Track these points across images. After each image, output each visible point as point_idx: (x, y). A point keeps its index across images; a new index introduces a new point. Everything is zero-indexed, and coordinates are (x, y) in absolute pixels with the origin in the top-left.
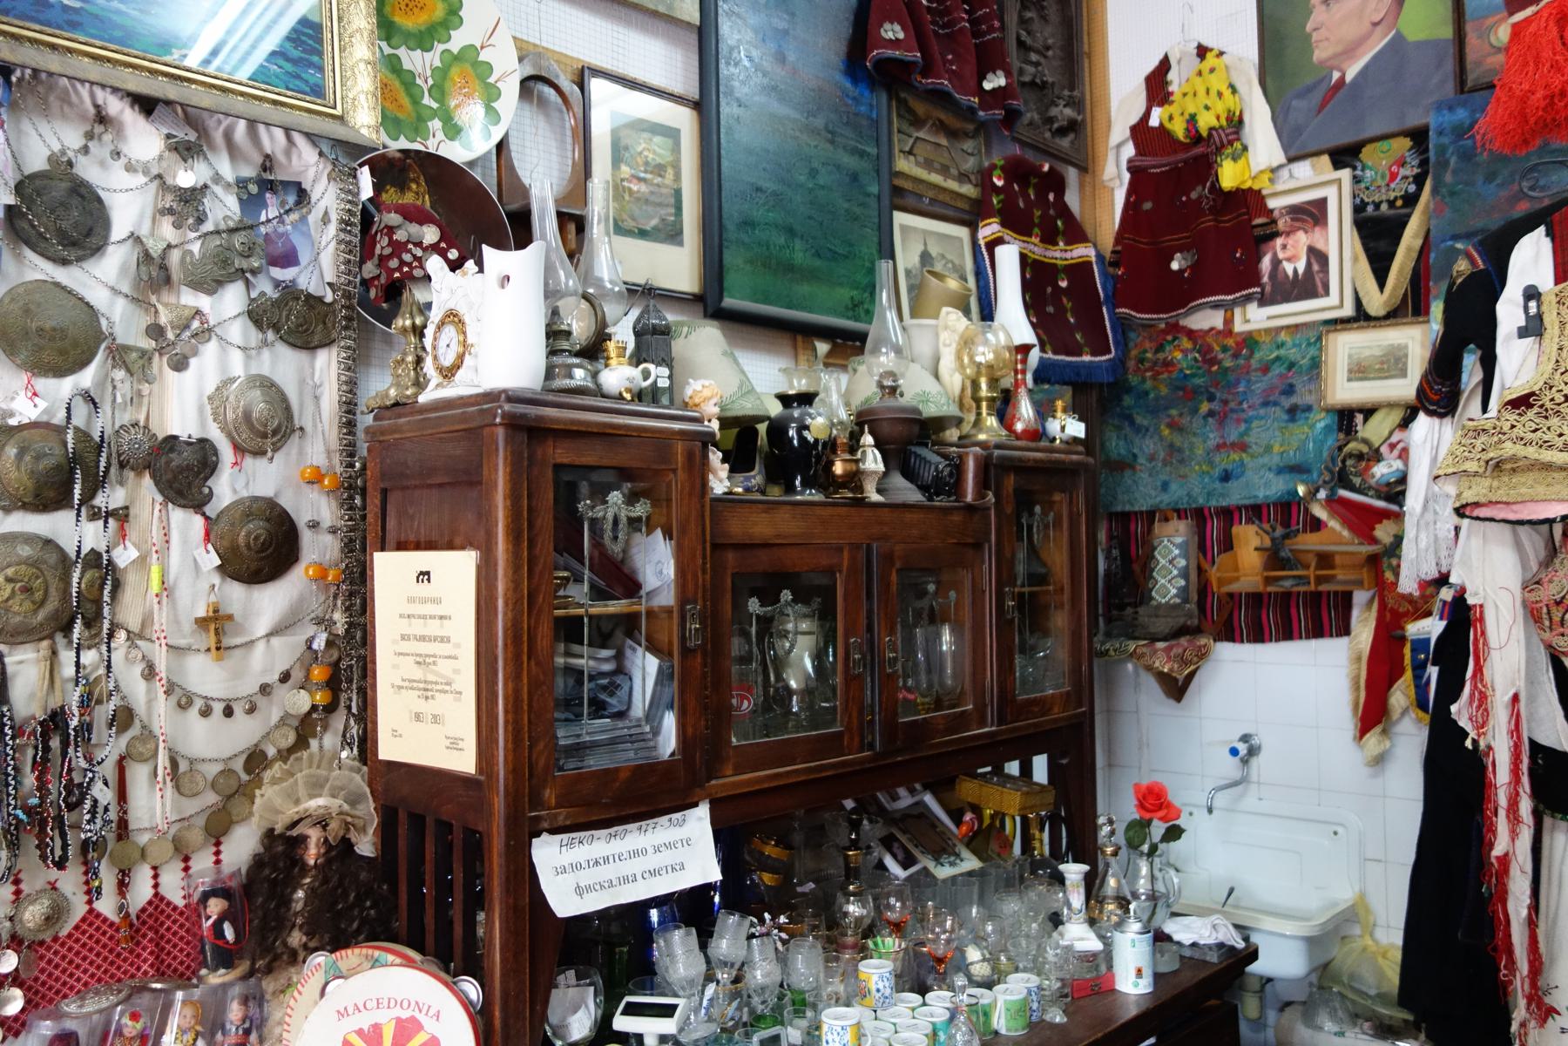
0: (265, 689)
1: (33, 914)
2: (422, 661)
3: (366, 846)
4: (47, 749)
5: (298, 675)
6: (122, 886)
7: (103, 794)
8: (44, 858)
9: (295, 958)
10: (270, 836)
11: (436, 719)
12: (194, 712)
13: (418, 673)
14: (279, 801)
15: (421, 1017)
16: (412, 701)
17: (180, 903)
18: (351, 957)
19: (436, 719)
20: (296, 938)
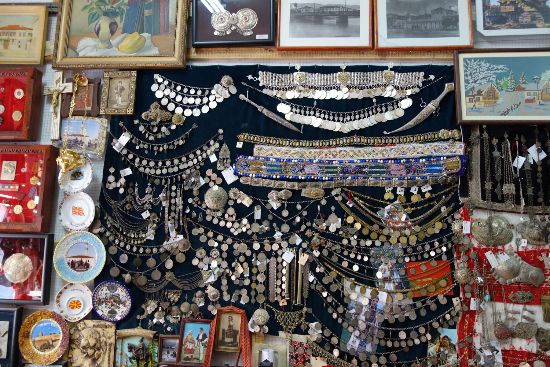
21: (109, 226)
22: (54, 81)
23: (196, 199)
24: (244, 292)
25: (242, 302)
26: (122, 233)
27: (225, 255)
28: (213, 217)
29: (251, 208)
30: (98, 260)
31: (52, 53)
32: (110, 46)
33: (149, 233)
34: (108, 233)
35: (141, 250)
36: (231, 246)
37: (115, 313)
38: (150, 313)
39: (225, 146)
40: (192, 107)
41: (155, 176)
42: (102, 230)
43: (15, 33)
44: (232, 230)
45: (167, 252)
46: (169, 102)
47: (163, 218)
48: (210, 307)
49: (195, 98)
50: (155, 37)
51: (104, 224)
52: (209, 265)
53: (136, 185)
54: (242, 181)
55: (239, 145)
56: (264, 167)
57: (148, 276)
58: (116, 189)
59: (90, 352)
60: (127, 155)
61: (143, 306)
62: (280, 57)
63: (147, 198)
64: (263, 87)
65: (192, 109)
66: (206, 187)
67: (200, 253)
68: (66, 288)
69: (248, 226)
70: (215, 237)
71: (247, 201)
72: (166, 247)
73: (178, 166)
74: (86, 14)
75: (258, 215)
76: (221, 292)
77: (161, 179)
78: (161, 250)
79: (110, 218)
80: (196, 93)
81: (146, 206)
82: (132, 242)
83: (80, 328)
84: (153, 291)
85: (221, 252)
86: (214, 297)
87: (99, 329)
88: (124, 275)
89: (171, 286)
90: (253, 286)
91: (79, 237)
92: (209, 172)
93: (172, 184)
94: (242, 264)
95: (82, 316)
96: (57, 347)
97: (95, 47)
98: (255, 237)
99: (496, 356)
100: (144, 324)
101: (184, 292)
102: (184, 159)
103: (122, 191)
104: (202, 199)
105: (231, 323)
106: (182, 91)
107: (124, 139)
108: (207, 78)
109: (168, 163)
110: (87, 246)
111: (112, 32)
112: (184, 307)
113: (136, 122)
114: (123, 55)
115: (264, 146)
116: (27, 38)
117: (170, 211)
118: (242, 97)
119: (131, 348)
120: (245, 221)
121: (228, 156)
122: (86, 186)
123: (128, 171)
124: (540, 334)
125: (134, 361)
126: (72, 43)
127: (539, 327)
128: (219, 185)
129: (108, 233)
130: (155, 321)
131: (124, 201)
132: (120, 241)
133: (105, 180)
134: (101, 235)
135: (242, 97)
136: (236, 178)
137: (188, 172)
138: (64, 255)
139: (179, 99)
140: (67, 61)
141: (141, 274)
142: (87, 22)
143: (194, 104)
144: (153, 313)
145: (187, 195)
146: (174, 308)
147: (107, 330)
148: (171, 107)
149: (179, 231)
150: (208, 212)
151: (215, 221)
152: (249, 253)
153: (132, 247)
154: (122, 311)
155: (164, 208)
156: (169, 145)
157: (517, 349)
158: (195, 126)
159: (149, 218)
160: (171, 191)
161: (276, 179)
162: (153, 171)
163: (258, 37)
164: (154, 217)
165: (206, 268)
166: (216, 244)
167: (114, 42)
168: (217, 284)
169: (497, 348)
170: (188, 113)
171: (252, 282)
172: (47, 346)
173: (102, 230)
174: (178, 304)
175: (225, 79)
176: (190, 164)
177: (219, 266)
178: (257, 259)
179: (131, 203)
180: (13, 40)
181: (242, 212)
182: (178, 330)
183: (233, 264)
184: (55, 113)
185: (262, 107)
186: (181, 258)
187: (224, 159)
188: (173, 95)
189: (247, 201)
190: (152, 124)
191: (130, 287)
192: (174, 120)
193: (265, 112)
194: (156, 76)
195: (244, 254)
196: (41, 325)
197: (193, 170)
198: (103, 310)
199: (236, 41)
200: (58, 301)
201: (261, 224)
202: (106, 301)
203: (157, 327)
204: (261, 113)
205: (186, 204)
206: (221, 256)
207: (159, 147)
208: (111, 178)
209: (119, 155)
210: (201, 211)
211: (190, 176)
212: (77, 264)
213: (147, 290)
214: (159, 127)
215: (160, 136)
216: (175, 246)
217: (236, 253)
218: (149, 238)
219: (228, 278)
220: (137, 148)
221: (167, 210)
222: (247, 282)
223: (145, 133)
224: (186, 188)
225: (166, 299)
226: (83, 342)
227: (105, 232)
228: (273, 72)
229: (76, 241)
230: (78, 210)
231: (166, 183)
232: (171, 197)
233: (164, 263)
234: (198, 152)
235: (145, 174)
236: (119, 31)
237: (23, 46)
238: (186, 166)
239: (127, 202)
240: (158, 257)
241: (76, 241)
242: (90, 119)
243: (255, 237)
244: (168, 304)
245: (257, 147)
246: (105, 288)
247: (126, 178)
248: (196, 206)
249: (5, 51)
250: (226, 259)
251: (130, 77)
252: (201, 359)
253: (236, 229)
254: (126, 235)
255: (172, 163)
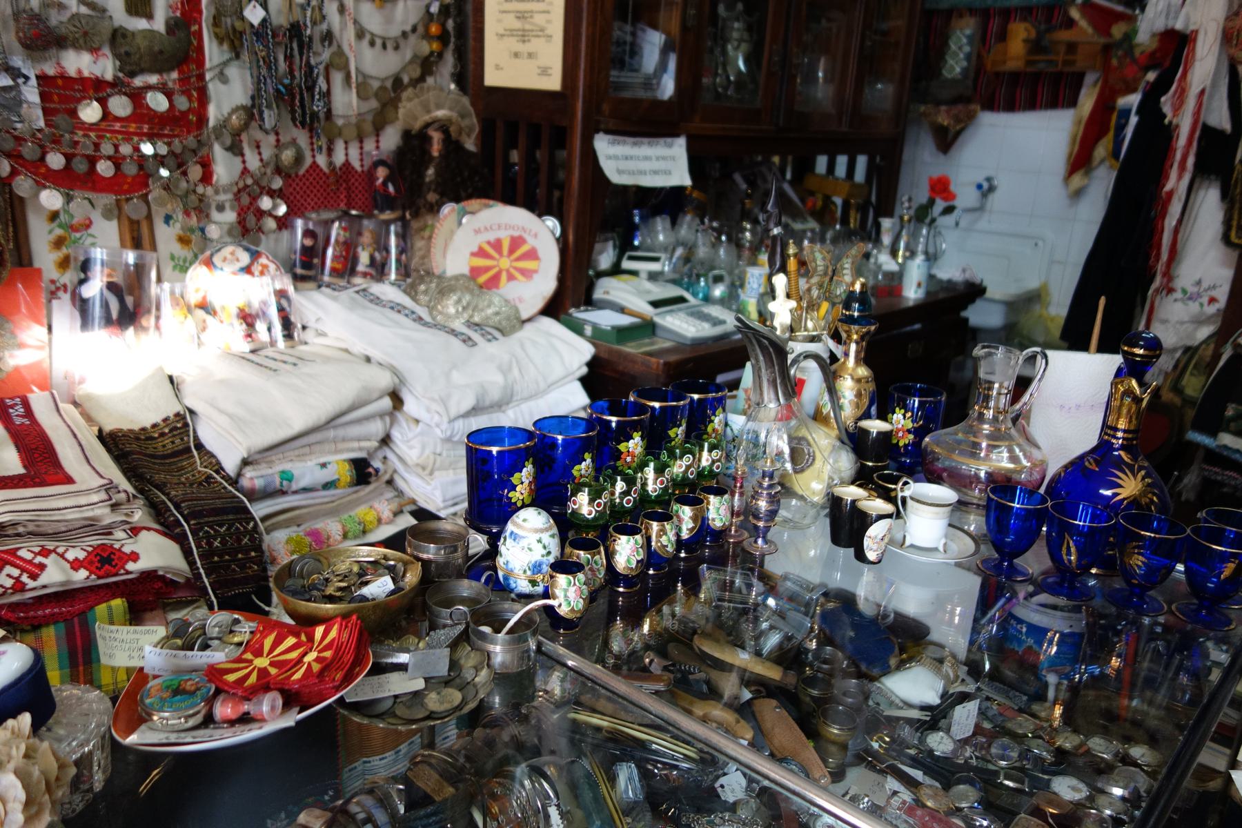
0: (404, 35)
1: (288, 155)
2: (521, 16)
3: (470, 145)
4: (292, 49)
5: (421, 29)
6: (330, 151)
7: (322, 83)
8: (294, 120)
9: (434, 209)
10: (407, 135)
11: (530, 55)
12: (365, 42)
13: (517, 25)
14: (413, 111)
15: (526, 236)
16: (514, 44)
17: (359, 169)
18: (474, 204)
19: (530, 55)
20: (432, 197)
99: (24, 89)
124: (120, 40)
127: (117, 24)
157: (72, 72)
169: (24, 71)
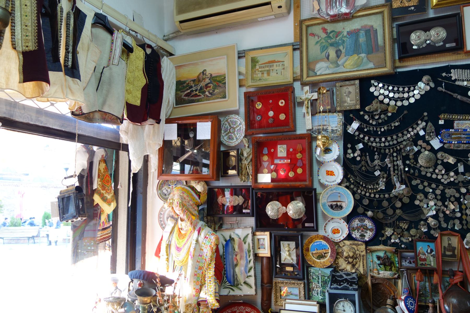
21: (352, 182)
22: (303, 93)
23: (412, 161)
24: (457, 222)
25: (456, 228)
26: (362, 185)
27: (439, 197)
28: (427, 172)
29: (456, 165)
30: (348, 203)
31: (299, 74)
32: (338, 66)
33: (381, 185)
34: (352, 186)
35: (377, 196)
36: (443, 191)
37: (365, 236)
38: (389, 236)
39: (430, 124)
40: (402, 99)
41: (379, 149)
42: (348, 184)
43: (273, 65)
44: (442, 180)
45: (396, 197)
46: (385, 98)
47: (389, 175)
48: (432, 232)
49: (403, 93)
50: (370, 56)
51: (348, 180)
52: (428, 204)
53: (367, 154)
54: (446, 146)
55: (441, 122)
56: (463, 136)
57: (384, 212)
58: (354, 158)
59: (350, 260)
60: (359, 135)
61: (383, 232)
62: (466, 57)
63: (376, 162)
64: (455, 80)
65: (402, 101)
66: (419, 152)
67: (420, 196)
68: (329, 221)
69: (455, 177)
70: (429, 185)
71: (451, 160)
72: (394, 193)
73: (396, 140)
74: (318, 47)
75: (461, 169)
76: (440, 222)
77: (385, 150)
78: (391, 195)
79: (352, 176)
80: (404, 90)
81: (377, 167)
82: (370, 191)
83: (341, 245)
84: (389, 222)
85: (436, 195)
86: (435, 225)
87: (354, 246)
88: (366, 212)
89: (400, 219)
90: (464, 217)
91: (334, 189)
92: (420, 142)
93: (394, 152)
94: (452, 203)
95: (342, 238)
96: (328, 257)
97: (328, 67)
98: (461, 184)
100: (385, 243)
101: (411, 222)
102: (400, 135)
103: (358, 159)
104: (417, 162)
105: (450, 242)
106: (393, 89)
107: (355, 125)
108: (412, 79)
109: (389, 138)
110: (339, 195)
111: (338, 57)
112: (413, 232)
113: (362, 113)
114: (348, 70)
115: (461, 122)
116: (281, 67)
117: (394, 170)
118: (440, 89)
119: (379, 258)
120: (452, 174)
121: (433, 130)
122: (336, 157)
123: (361, 146)
125: (381, 266)
126: (312, 67)
128: (428, 151)
129: (352, 186)
130: (392, 241)
131: (360, 165)
132: (362, 191)
133: (345, 152)
134: (347, 187)
135: (440, 89)
136: (442, 145)
137: (404, 143)
138: (325, 201)
139: (391, 95)
140: (309, 79)
141: (379, 212)
142: (319, 52)
143: (403, 97)
144: (391, 236)
145: (405, 158)
146: (406, 233)
147: (359, 246)
148: (386, 101)
149: (402, 182)
150: (422, 169)
151: (429, 175)
152: (457, 195)
153: (370, 194)
154: (368, 235)
155: (390, 168)
156: (388, 126)
158: (405, 112)
159: (379, 175)
160: (393, 157)
161: (464, 143)
162: (378, 145)
163: (447, 45)
164: (383, 174)
165: (425, 206)
166: (431, 190)
167: (340, 63)
168: (435, 217)
170: (399, 104)
171: (462, 214)
172: (321, 257)
173: (348, 184)
174: (408, 230)
175: (425, 78)
176: (405, 138)
177: (435, 205)
178: (464, 199)
179: (365, 166)
180: (273, 70)
181: (448, 167)
182: (411, 246)
183: (446, 203)
184: (308, 113)
185: (457, 95)
186: (406, 200)
187: (430, 133)
188: (386, 93)
189: (451, 160)
190: (375, 113)
191: (372, 219)
192: (389, 110)
193: (459, 97)
194: (372, 82)
195: (454, 196)
196: (316, 244)
197: (408, 142)
198: (356, 234)
199: (430, 51)
200: (325, 229)
201: (464, 175)
202: (358, 228)
203: (394, 244)
204: (456, 99)
205: (405, 165)
206: (436, 198)
207: (381, 128)
208: (350, 151)
209: (353, 136)
210: (417, 168)
211: (406, 146)
212: (334, 206)
213: (384, 222)
214: (380, 114)
215: (380, 121)
216: (401, 192)
217: (447, 196)
218: (382, 188)
219: (444, 212)
220: (366, 130)
221: (392, 169)
222: (459, 215)
223: (370, 120)
224: (404, 154)
225: (399, 227)
226: (345, 254)
227: (350, 185)
228: (462, 69)
229: (332, 192)
230: (330, 172)
231: (389, 152)
232: (394, 161)
233: (394, 204)
234: (410, 130)
235: (374, 147)
236: (343, 55)
237: (279, 73)
238: (402, 139)
239: (363, 166)
240: (389, 200)
241: (332, 192)
242: (330, 114)
243: (461, 184)
244: (400, 230)
245: (456, 122)
246: (357, 220)
247: (360, 150)
248: (412, 165)
249: (268, 77)
250: (440, 200)
251: (354, 84)
252: (432, 265)
253: (446, 180)
254: (365, 187)
255: (392, 138)
